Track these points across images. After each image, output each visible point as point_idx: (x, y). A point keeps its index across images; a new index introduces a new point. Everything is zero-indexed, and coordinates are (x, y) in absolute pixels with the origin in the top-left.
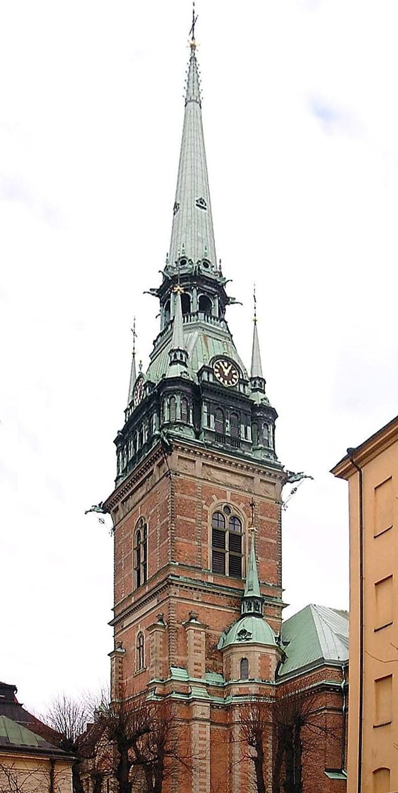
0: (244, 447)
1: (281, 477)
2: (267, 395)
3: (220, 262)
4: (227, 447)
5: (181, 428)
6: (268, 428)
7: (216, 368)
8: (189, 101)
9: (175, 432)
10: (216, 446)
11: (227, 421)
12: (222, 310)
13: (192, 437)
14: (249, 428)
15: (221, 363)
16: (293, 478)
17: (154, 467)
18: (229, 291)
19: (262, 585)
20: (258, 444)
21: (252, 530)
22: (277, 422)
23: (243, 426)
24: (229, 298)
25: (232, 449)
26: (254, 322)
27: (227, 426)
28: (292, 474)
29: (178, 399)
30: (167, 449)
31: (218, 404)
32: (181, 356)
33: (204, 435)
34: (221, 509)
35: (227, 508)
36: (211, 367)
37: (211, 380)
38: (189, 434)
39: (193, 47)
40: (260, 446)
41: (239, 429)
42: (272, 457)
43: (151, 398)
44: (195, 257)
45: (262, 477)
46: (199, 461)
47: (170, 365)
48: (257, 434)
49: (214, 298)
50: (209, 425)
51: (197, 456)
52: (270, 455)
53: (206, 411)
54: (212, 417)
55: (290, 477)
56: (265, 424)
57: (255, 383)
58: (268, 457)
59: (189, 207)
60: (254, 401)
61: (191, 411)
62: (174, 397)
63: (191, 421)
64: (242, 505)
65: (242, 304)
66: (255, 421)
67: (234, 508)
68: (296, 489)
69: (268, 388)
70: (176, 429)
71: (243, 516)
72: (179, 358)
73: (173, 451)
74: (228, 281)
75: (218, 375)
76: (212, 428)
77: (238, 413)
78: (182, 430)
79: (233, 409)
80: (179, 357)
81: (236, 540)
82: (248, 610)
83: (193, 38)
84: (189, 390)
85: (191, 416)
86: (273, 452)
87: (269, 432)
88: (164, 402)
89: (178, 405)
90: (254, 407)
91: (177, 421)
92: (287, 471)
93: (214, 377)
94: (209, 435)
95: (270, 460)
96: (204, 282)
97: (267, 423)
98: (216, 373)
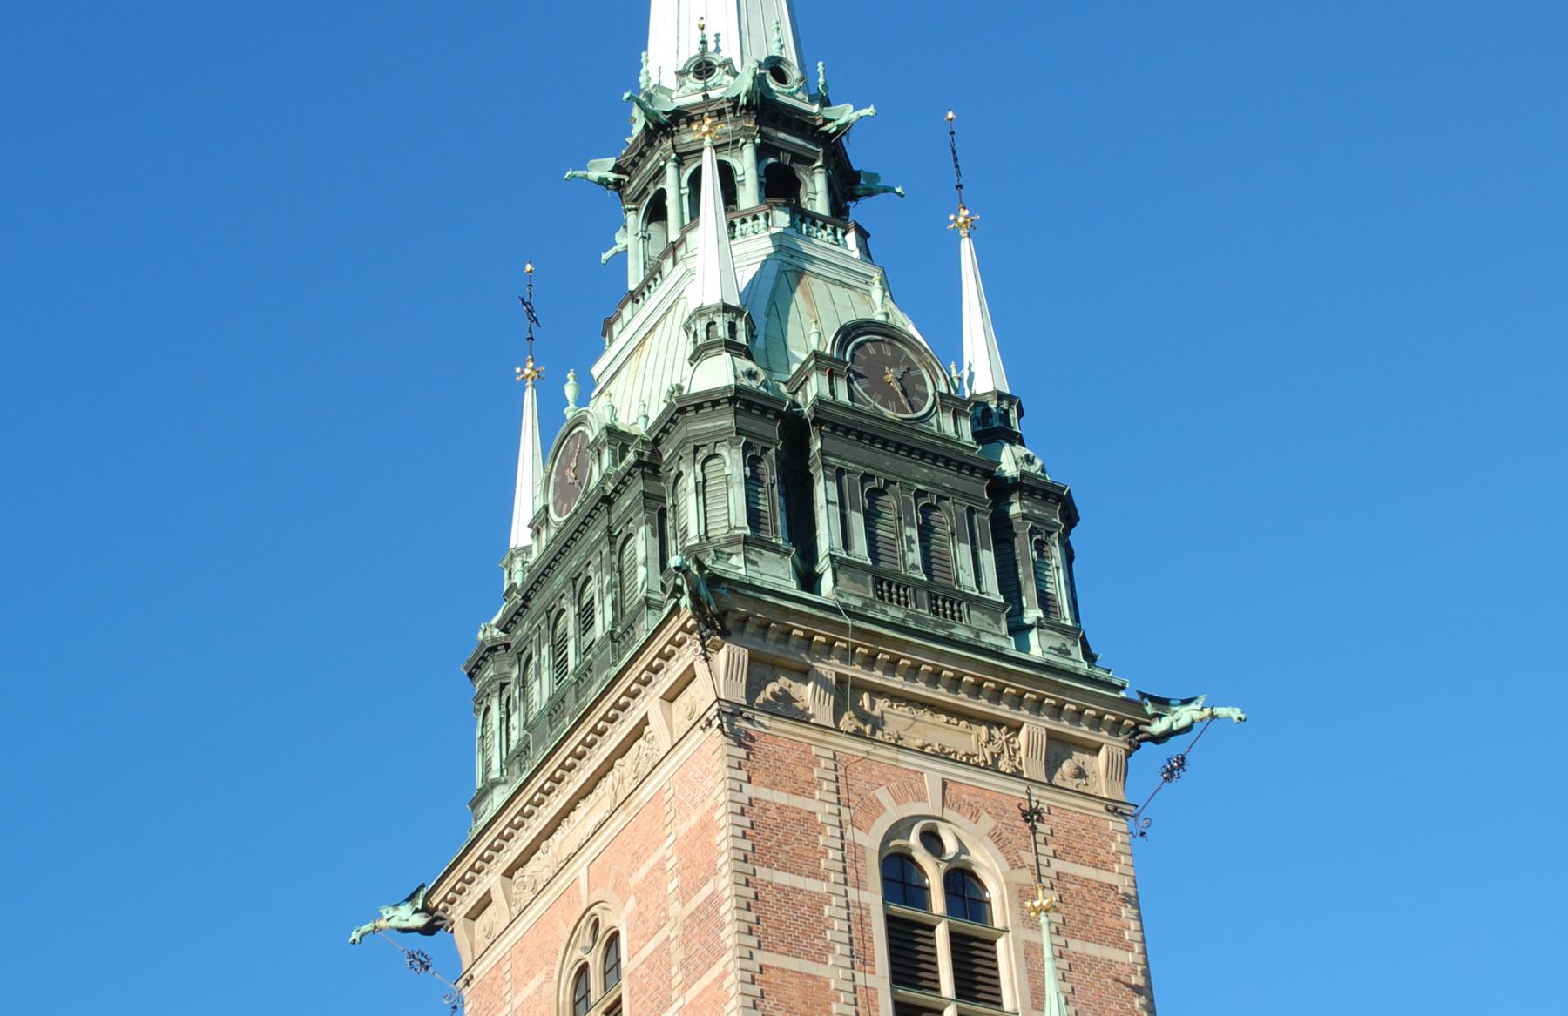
0: (978, 618)
4: (918, 619)
5: (753, 556)
10: (880, 616)
13: (791, 586)
23: (964, 552)
24: (857, 174)
25: (937, 625)
27: (911, 550)
37: (843, 397)
38: (777, 574)
42: (1077, 652)
49: (812, 174)
52: (1069, 647)
58: (1064, 652)
78: (754, 563)
88: (680, 475)
94: (852, 579)
95: (1071, 663)
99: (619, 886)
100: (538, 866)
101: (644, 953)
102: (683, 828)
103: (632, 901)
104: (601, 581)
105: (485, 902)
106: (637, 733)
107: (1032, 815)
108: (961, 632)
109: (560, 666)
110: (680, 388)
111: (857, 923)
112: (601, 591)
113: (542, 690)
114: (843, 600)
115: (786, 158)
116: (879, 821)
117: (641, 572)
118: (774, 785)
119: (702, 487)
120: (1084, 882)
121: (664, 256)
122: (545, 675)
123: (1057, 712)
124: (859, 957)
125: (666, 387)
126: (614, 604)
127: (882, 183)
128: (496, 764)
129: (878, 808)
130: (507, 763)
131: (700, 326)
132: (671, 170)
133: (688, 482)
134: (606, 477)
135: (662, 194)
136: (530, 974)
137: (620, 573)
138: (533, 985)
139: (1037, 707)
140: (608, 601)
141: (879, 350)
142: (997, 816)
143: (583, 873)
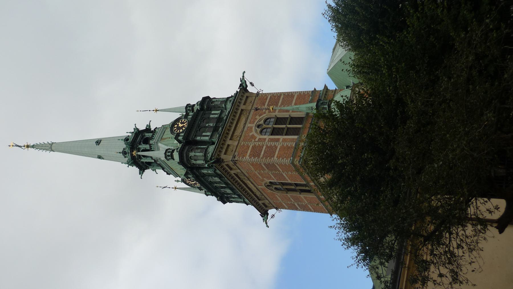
0: (223, 115)
1: (243, 93)
2: (195, 103)
3: (128, 133)
5: (208, 152)
6: (214, 101)
7: (177, 131)
8: (51, 149)
9: (209, 155)
11: (207, 125)
12: (152, 132)
13: (214, 146)
14: (213, 112)
15: (175, 129)
16: (244, 85)
17: (232, 172)
18: (142, 127)
19: (311, 102)
20: (223, 107)
21: (272, 109)
22: (211, 97)
23: (211, 116)
24: (146, 128)
26: (157, 111)
28: (241, 85)
29: (192, 154)
30: (219, 161)
31: (197, 130)
32: (169, 152)
33: (213, 139)
34: (259, 130)
35: (258, 126)
36: (176, 134)
38: (211, 148)
39: (28, 146)
40: (223, 106)
41: (213, 118)
42: (231, 99)
43: (194, 174)
44: (123, 146)
45: (242, 104)
46: (229, 142)
47: (174, 160)
48: (216, 108)
49: (145, 136)
50: (207, 136)
51: (225, 143)
52: (230, 100)
53: (200, 137)
54: (204, 134)
55: (243, 86)
56: (211, 104)
57: (189, 110)
58: (230, 101)
59: (100, 150)
60: (197, 109)
61: (199, 147)
62: (191, 156)
63: (205, 147)
64: (257, 117)
65: (151, 121)
66: (210, 109)
67: (259, 122)
68: (251, 83)
69: (192, 104)
70: (208, 156)
71: (265, 116)
72: (169, 154)
73: (221, 158)
74: (136, 127)
75: (181, 131)
76: (209, 134)
77: (203, 119)
78: (209, 152)
79: (201, 122)
80: (169, 154)
81: (279, 120)
82: (326, 110)
83: (24, 146)
84: (187, 147)
85: (202, 147)
86: (228, 98)
87: (216, 101)
89: (195, 154)
90: (202, 108)
91: (203, 155)
92: (239, 88)
93: (182, 132)
96: (136, 141)
97: (211, 102)
98: (180, 131)
99: (263, 180)
100: (258, 194)
101: (274, 178)
102: (253, 169)
103: (265, 179)
104: (211, 179)
105: (264, 204)
106: (237, 175)
107: (257, 109)
108: (225, 118)
109: (224, 188)
110: (178, 162)
111: (271, 140)
112: (212, 179)
113: (229, 191)
114: (217, 138)
115: (142, 140)
116: (255, 135)
117: (209, 172)
118: (247, 152)
119: (196, 160)
120: (269, 101)
121: (157, 163)
122: (226, 190)
123: (240, 103)
124: (278, 140)
125: (178, 164)
126: (215, 177)
127: (149, 124)
128: (241, 200)
129: (253, 135)
130: (241, 198)
131: (168, 158)
132: (142, 160)
133: (194, 162)
134: (193, 177)
135: (146, 162)
136: (276, 197)
137: (210, 175)
138: (278, 197)
139: (238, 106)
140: (214, 178)
141: (176, 127)
142: (256, 115)
143: (259, 187)
